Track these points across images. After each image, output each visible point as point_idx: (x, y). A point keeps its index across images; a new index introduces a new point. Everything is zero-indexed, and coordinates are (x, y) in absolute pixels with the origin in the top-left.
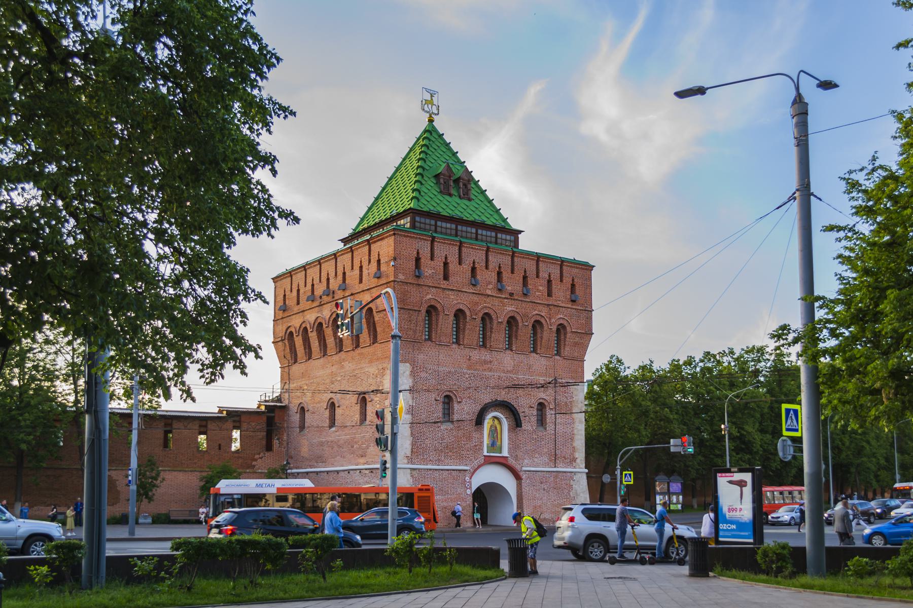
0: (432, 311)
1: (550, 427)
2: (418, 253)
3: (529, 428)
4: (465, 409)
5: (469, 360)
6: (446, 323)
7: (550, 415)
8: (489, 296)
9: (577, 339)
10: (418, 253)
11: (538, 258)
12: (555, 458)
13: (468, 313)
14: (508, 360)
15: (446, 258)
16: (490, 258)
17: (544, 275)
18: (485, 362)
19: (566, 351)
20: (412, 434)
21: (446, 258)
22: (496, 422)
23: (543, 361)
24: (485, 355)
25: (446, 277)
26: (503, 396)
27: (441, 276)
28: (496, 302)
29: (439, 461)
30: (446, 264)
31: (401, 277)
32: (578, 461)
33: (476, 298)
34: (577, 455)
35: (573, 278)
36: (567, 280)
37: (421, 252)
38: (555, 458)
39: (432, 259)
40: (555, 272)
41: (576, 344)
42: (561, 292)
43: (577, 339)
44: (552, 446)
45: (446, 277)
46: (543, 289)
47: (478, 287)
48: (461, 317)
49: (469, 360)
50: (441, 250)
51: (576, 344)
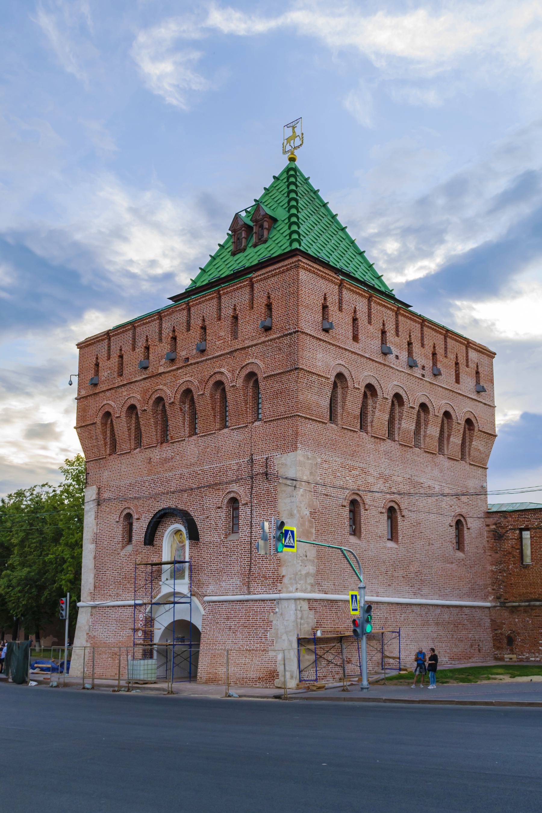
3: (216, 538)
4: (140, 528)
5: (150, 463)
7: (244, 512)
8: (160, 374)
9: (277, 386)
12: (249, 579)
13: (138, 407)
14: (191, 448)
19: (266, 408)
20: (95, 567)
24: (167, 451)
27: (116, 375)
28: (168, 378)
31: (83, 393)
32: (286, 580)
33: (147, 383)
34: (283, 571)
38: (249, 579)
39: (109, 359)
41: (278, 394)
43: (277, 386)
44: (246, 562)
47: (150, 369)
49: (150, 463)
51: (278, 394)
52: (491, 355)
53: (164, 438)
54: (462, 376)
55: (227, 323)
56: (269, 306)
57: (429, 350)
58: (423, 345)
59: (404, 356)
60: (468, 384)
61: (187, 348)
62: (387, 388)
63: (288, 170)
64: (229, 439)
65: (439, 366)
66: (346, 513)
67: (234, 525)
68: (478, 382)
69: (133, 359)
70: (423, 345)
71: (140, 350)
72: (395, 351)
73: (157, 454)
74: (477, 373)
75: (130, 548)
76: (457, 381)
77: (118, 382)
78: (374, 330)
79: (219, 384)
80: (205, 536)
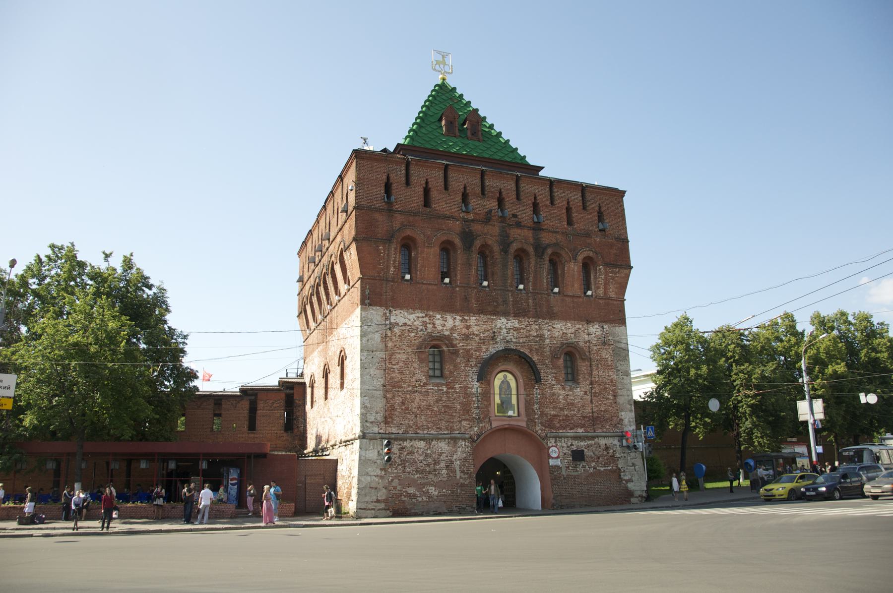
0: (408, 245)
2: (388, 178)
6: (428, 258)
10: (388, 178)
11: (552, 183)
15: (427, 183)
16: (487, 183)
17: (560, 202)
21: (427, 183)
22: (510, 376)
25: (427, 203)
30: (427, 191)
35: (601, 209)
37: (392, 176)
40: (576, 197)
42: (584, 221)
45: (427, 203)
48: (452, 252)
50: (419, 175)
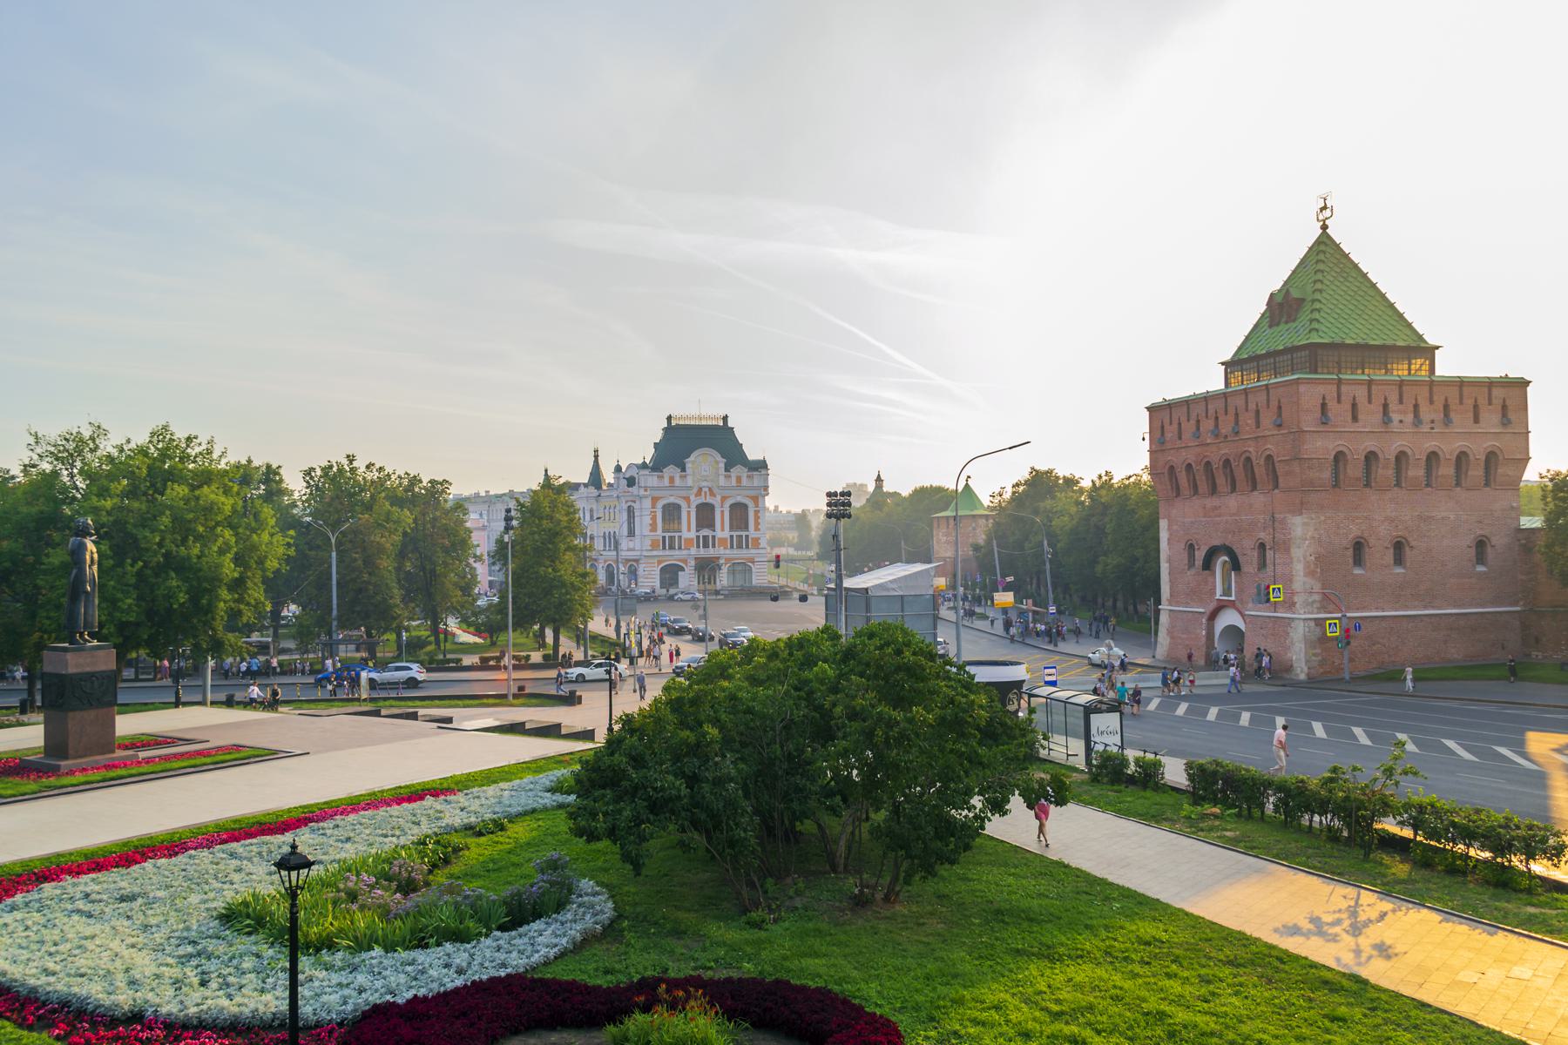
1: (1270, 568)
4: (1200, 555)
7: (1269, 554)
14: (1232, 502)
18: (1216, 508)
23: (1262, 498)
26: (1229, 540)
29: (1187, 604)
33: (1198, 450)
36: (1274, 404)
46: (1251, 422)
52: (1524, 384)
53: (1213, 490)
54: (1483, 416)
55: (1252, 414)
56: (1280, 408)
57: (1439, 404)
58: (1431, 402)
59: (1410, 418)
60: (1491, 420)
61: (1226, 428)
62: (1389, 451)
63: (1318, 242)
64: (1258, 499)
65: (1452, 415)
66: (1350, 552)
67: (1262, 564)
68: (1504, 415)
69: (1189, 428)
70: (1431, 402)
71: (1193, 422)
72: (1395, 417)
73: (1210, 502)
74: (1504, 407)
75: (1193, 571)
76: (1476, 420)
77: (1179, 444)
78: (1376, 407)
79: (1248, 459)
80: (1245, 568)
